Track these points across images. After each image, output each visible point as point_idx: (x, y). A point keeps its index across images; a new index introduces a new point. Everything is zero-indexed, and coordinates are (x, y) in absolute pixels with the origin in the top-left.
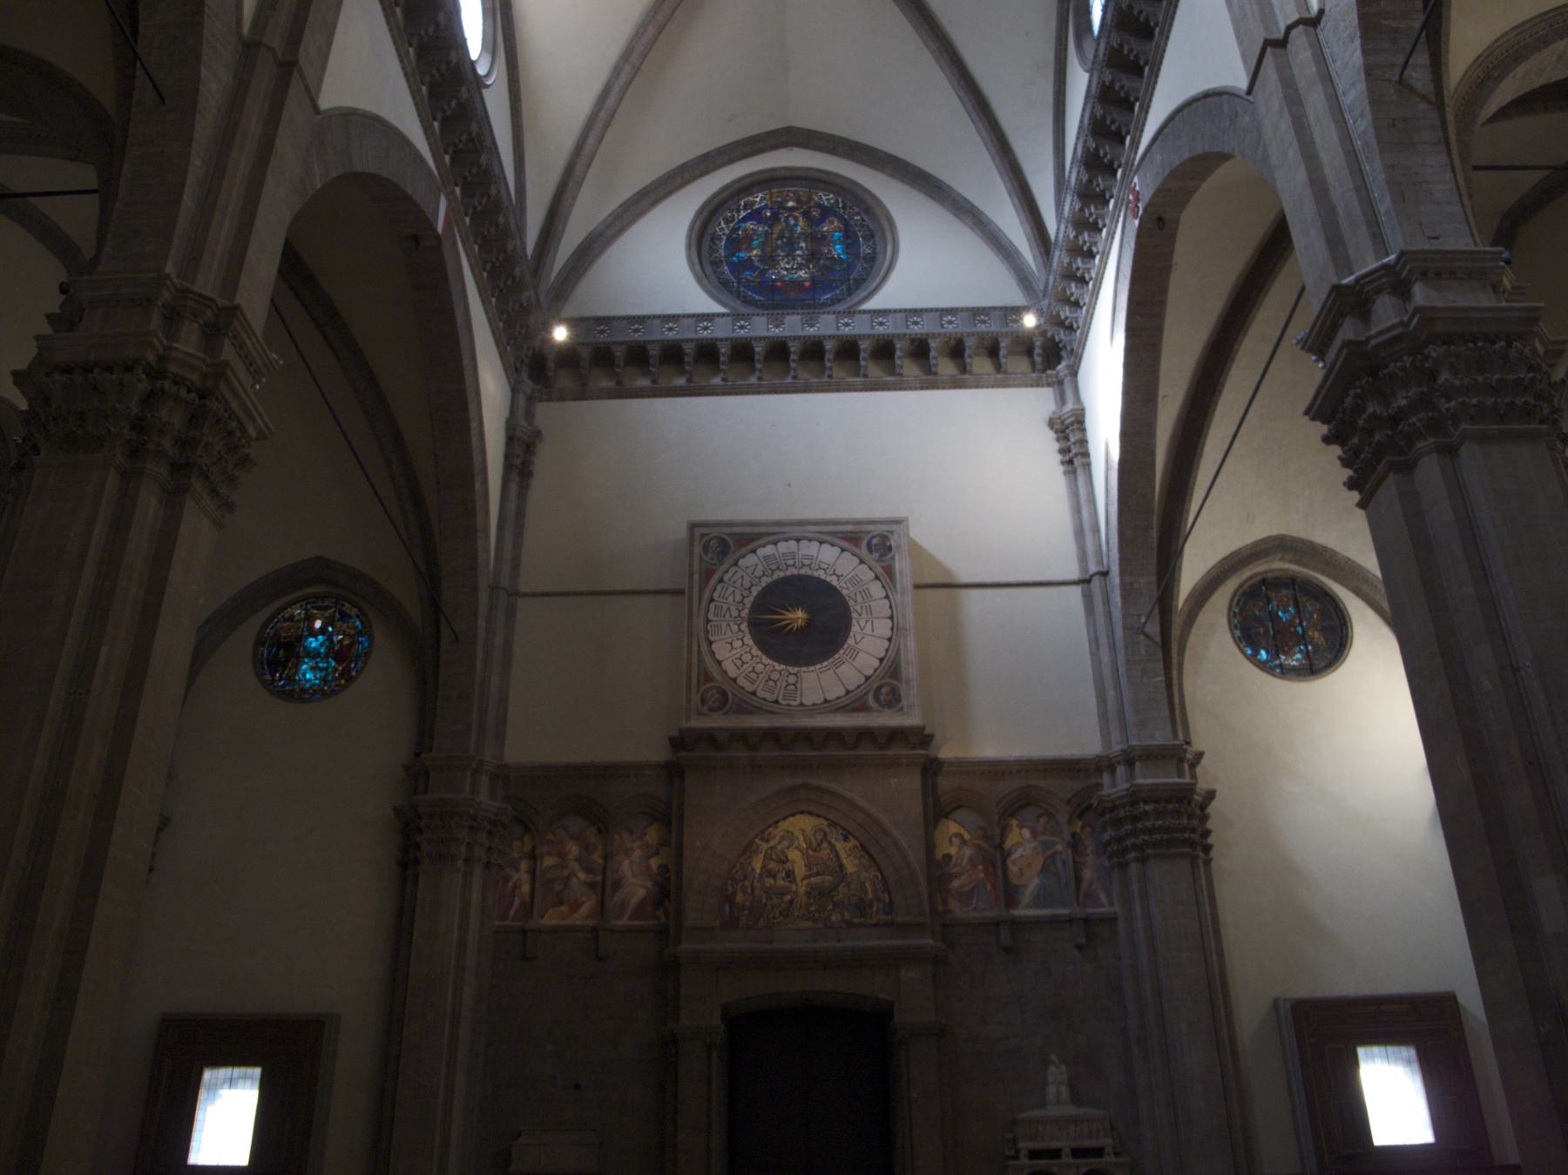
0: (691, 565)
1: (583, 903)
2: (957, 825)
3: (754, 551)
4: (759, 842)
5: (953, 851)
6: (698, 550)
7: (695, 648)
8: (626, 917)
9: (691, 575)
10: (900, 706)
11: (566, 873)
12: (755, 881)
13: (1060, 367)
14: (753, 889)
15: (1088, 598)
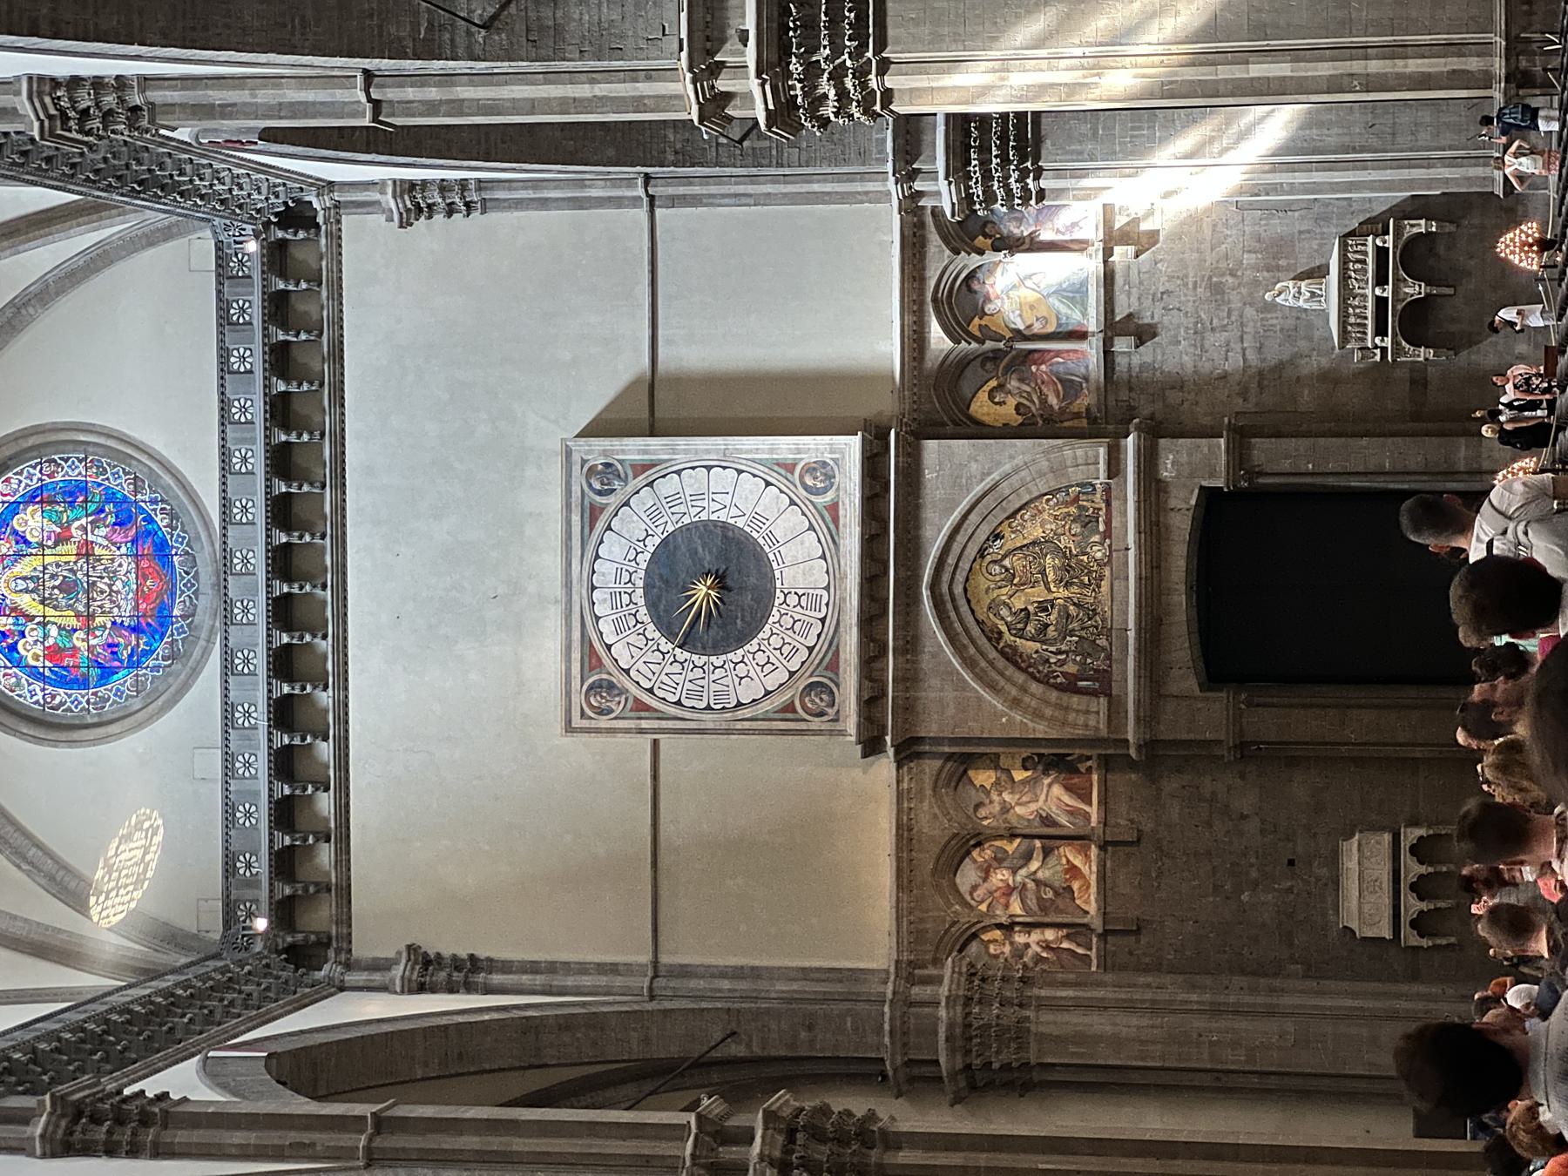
0: (627, 731)
1: (1068, 861)
2: (980, 394)
3: (609, 647)
4: (1002, 644)
5: (1012, 402)
6: (603, 722)
7: (747, 725)
8: (1087, 808)
9: (641, 731)
10: (831, 463)
11: (1031, 885)
12: (1053, 649)
13: (316, 205)
14: (1060, 652)
15: (673, 202)
